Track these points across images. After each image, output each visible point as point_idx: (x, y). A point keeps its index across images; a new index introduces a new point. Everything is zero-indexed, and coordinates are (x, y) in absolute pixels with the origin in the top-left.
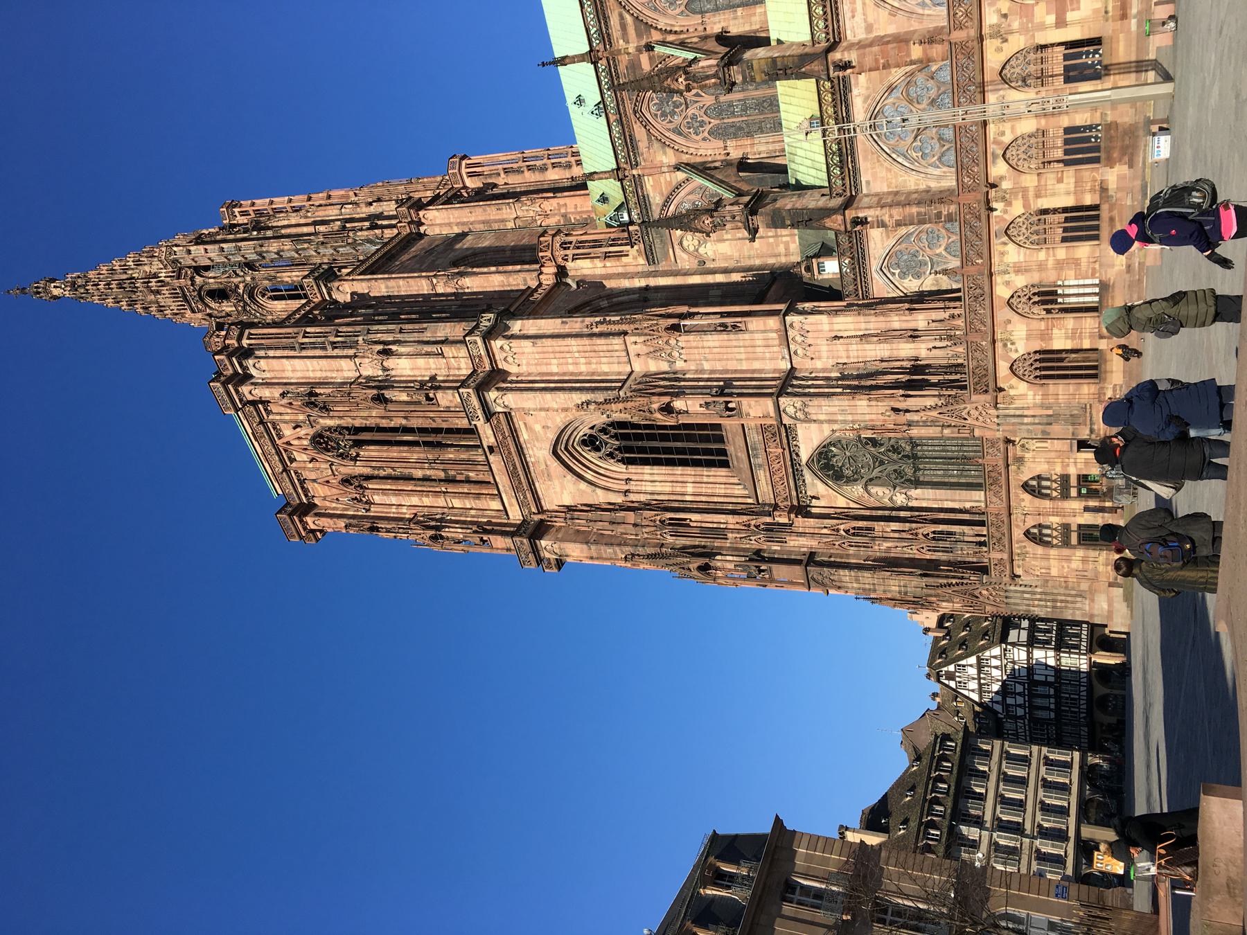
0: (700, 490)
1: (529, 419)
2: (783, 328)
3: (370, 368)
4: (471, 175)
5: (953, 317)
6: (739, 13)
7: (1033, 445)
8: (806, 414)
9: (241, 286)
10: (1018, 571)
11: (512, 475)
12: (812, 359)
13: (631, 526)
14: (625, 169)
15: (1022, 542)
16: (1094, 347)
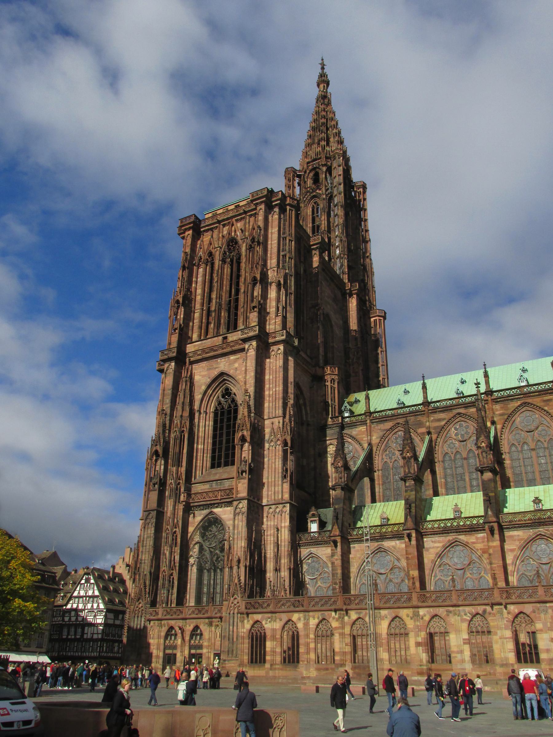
0: (199, 452)
1: (241, 361)
2: (284, 501)
3: (272, 275)
4: (375, 321)
5: (286, 590)
6: (442, 480)
7: (218, 631)
8: (239, 514)
9: (320, 192)
10: (152, 623)
11: (212, 349)
12: (267, 517)
13: (181, 414)
14: (370, 416)
15: (168, 625)
16: (267, 662)
